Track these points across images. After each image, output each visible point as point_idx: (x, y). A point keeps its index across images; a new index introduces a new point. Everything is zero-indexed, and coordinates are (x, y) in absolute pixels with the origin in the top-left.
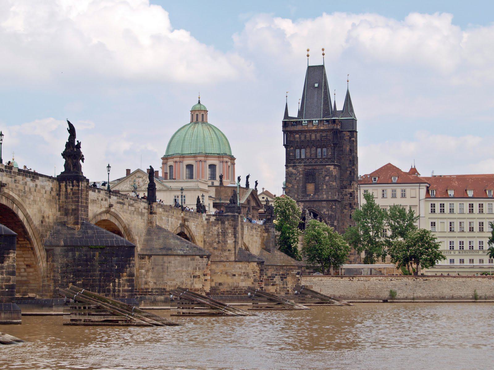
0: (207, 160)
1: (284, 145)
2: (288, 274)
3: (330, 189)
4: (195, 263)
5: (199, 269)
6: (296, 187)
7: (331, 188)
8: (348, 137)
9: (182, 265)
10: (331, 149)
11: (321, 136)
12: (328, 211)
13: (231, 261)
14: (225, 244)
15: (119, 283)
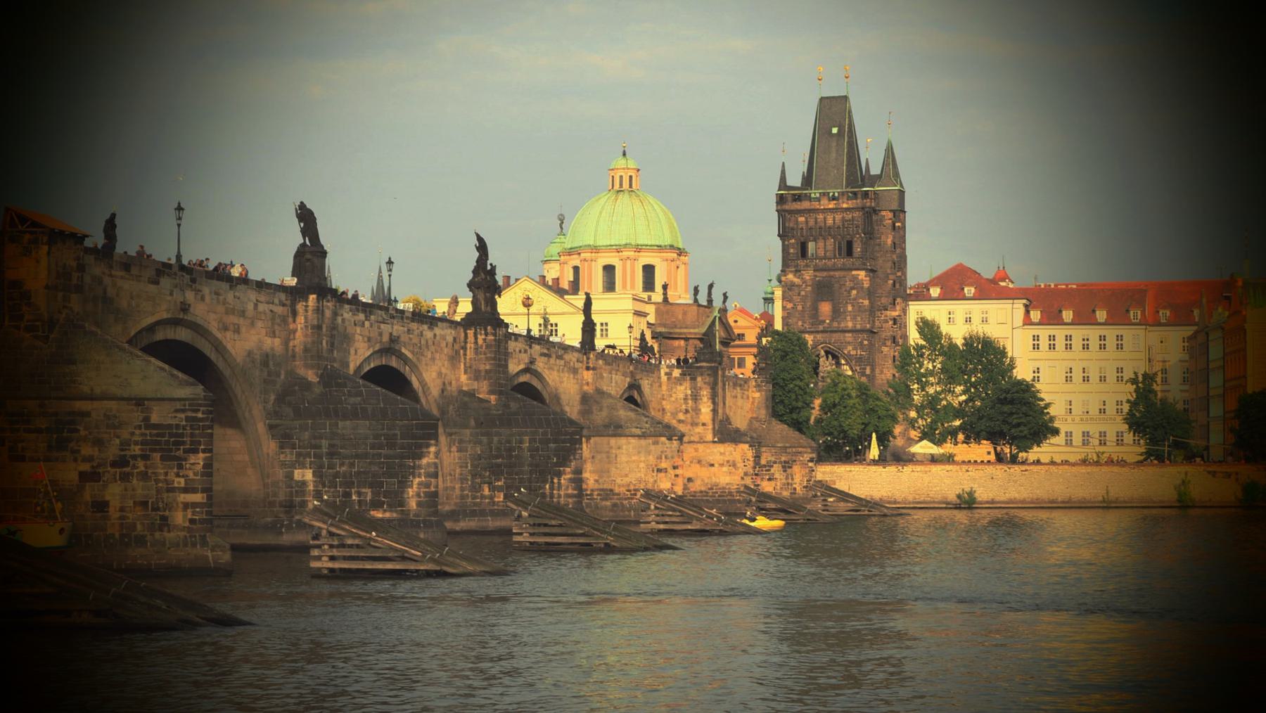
0: (639, 256)
1: (779, 235)
2: (795, 461)
3: (859, 311)
4: (659, 448)
5: (666, 457)
6: (800, 308)
7: (860, 309)
8: (890, 221)
9: (639, 452)
10: (861, 241)
11: (843, 220)
12: (855, 349)
13: (707, 442)
14: (697, 414)
15: (559, 483)
